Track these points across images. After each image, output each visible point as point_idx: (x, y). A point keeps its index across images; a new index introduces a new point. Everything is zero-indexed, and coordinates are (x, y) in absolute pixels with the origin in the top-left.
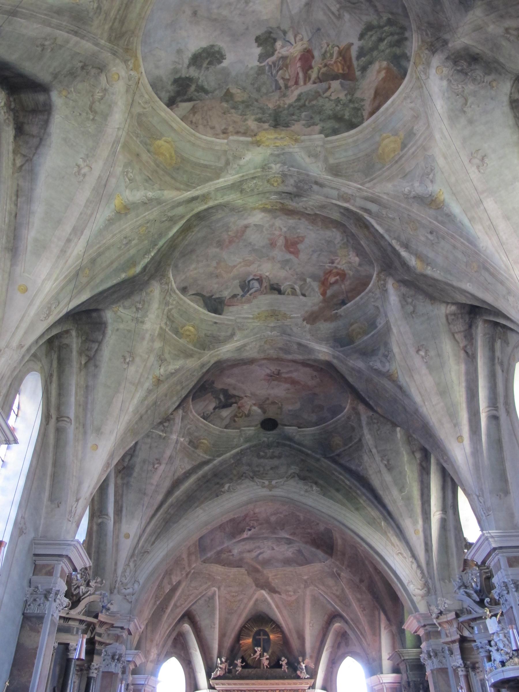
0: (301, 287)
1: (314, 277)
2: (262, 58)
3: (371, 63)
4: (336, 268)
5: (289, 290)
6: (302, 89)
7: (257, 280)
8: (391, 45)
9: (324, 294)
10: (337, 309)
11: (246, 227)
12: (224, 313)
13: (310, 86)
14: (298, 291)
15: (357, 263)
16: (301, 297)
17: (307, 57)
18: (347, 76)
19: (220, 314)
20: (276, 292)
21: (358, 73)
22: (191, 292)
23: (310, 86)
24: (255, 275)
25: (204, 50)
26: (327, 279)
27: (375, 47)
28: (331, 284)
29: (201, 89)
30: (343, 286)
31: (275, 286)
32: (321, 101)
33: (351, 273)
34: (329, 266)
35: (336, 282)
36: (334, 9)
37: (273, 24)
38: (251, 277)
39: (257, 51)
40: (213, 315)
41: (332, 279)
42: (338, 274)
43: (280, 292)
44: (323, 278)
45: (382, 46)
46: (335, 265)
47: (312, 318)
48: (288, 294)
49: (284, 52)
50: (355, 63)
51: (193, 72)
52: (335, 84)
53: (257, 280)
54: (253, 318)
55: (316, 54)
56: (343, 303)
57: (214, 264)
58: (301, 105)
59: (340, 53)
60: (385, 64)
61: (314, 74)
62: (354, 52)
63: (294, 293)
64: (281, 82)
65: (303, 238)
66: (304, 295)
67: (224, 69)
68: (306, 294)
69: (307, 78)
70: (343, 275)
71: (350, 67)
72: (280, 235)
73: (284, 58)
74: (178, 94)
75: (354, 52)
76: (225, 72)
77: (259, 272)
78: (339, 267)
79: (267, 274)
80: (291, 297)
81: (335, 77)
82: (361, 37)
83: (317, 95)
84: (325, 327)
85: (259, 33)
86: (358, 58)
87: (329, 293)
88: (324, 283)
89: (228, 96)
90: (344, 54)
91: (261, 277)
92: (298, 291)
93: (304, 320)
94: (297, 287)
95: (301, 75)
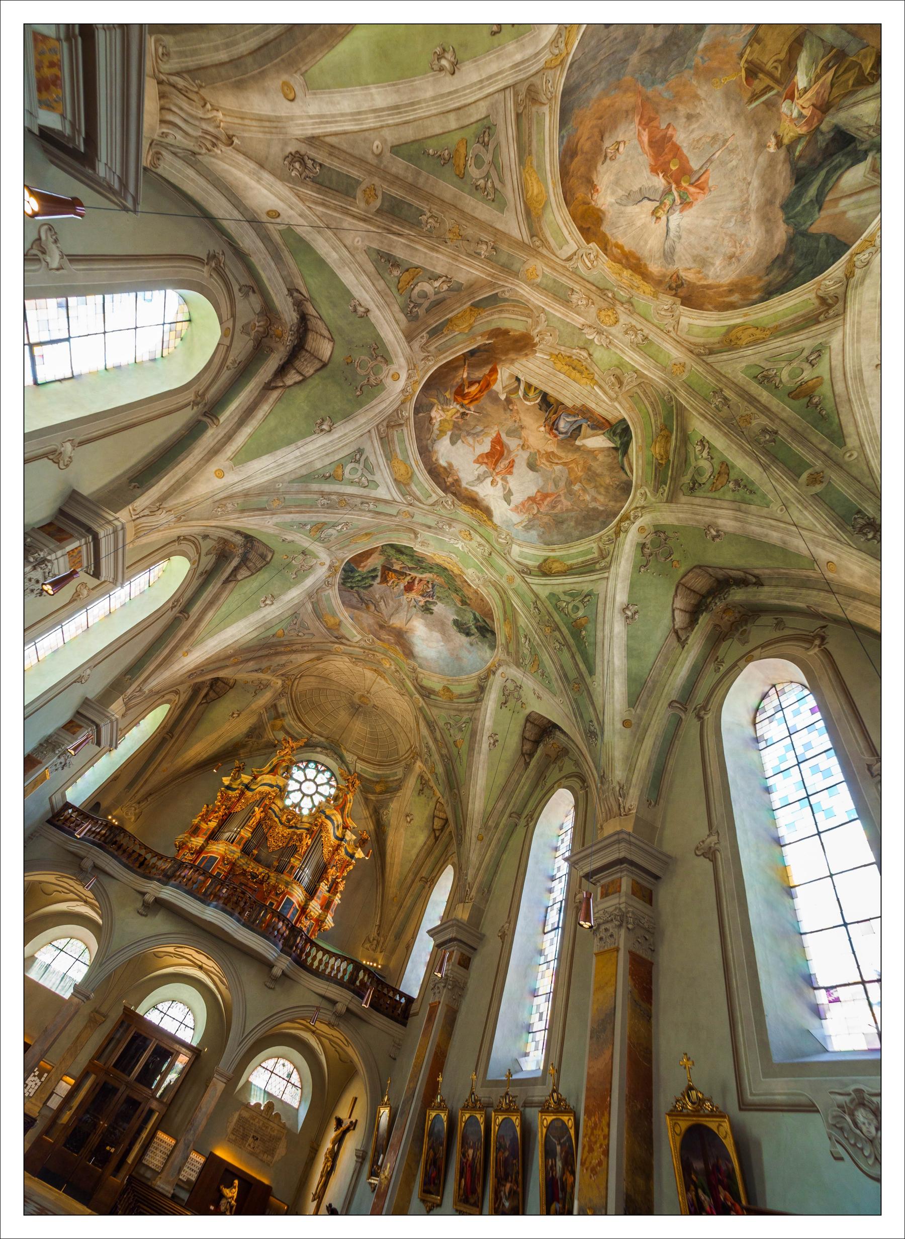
0: (517, 389)
1: (495, 398)
2: (434, 603)
3: (369, 572)
4: (462, 406)
5: (531, 394)
6: (421, 576)
7: (557, 429)
8: (353, 577)
9: (494, 371)
10: (485, 345)
11: (516, 509)
12: (620, 418)
13: (413, 574)
14: (522, 387)
15: (435, 409)
16: (522, 379)
17: (409, 588)
18: (387, 569)
19: (624, 420)
20: (549, 399)
21: (380, 568)
22: (624, 477)
23: (413, 574)
24: (556, 436)
25: (460, 632)
26: (480, 391)
27: (363, 579)
28: (479, 382)
29: (475, 618)
30: (465, 375)
31: (544, 407)
32: (410, 565)
33: (448, 395)
34: (469, 409)
35: (471, 384)
36: (382, 603)
37: (420, 614)
38: (561, 436)
39: (435, 609)
40: (632, 428)
41: (474, 389)
42: (464, 396)
43: (545, 396)
44: (485, 393)
45: (359, 578)
46: (462, 410)
47: (522, 344)
48: (536, 389)
49: (420, 598)
50: (379, 574)
51: (474, 630)
52: (396, 567)
53: (557, 429)
54: (597, 383)
55: (402, 587)
56: (472, 353)
57: (576, 487)
58: (424, 569)
59: (387, 582)
60: (360, 569)
61: (408, 578)
62: (378, 580)
63: (529, 386)
64: (430, 586)
65: (477, 461)
66: (518, 379)
67: (458, 615)
68: (514, 380)
69: (414, 579)
70: (460, 393)
71: (383, 573)
72: (497, 474)
73: (422, 595)
74: (487, 630)
75: (378, 580)
76: (458, 614)
77: (548, 436)
78: (458, 407)
79: (542, 429)
80: (535, 382)
81: (395, 571)
82: (371, 585)
83: (411, 569)
84: (514, 323)
85: (429, 616)
86: (377, 576)
87: (486, 370)
88: (486, 385)
89: (464, 603)
90: (384, 580)
91: (551, 429)
92: (522, 387)
93: (535, 345)
94: (521, 393)
95: (416, 582)
